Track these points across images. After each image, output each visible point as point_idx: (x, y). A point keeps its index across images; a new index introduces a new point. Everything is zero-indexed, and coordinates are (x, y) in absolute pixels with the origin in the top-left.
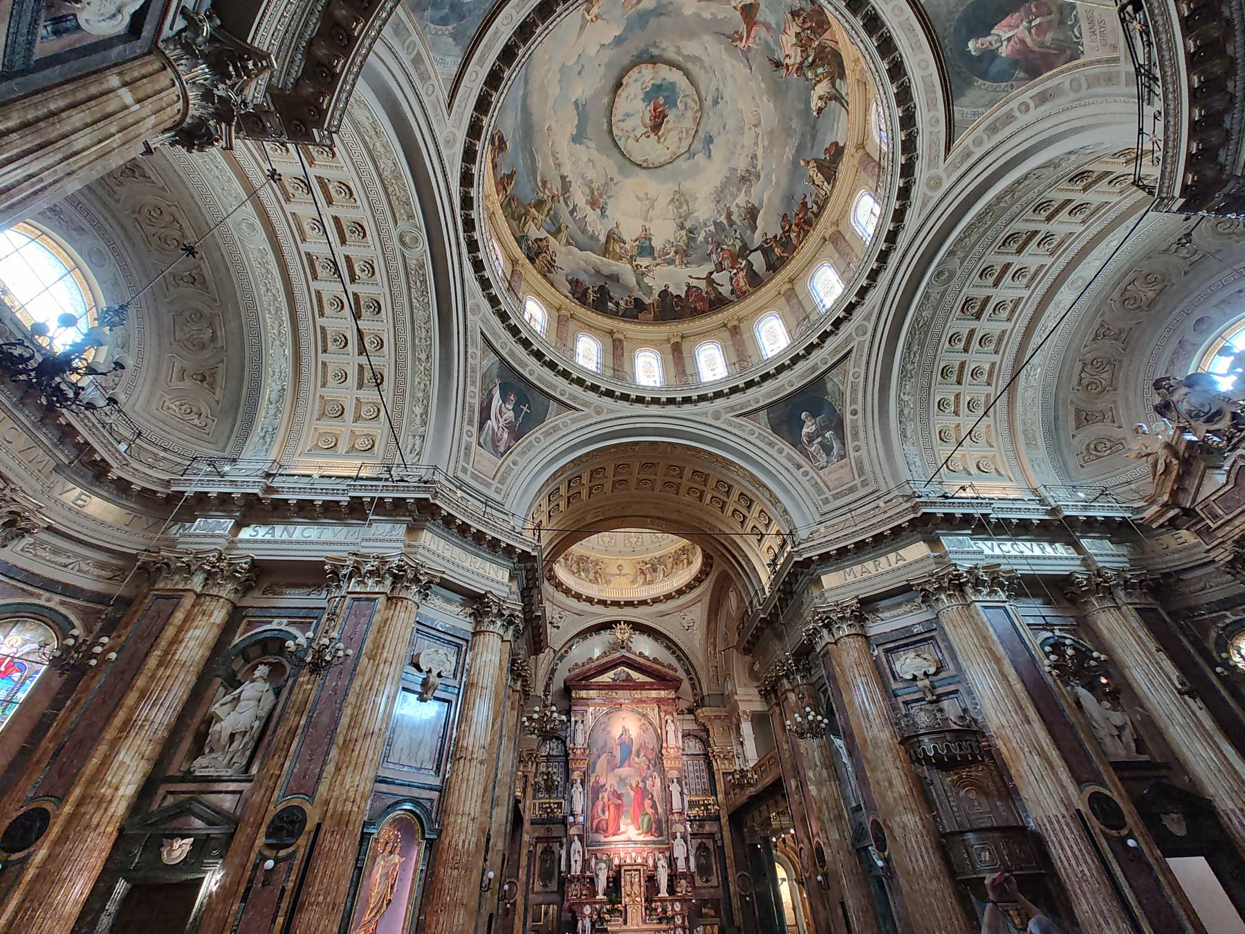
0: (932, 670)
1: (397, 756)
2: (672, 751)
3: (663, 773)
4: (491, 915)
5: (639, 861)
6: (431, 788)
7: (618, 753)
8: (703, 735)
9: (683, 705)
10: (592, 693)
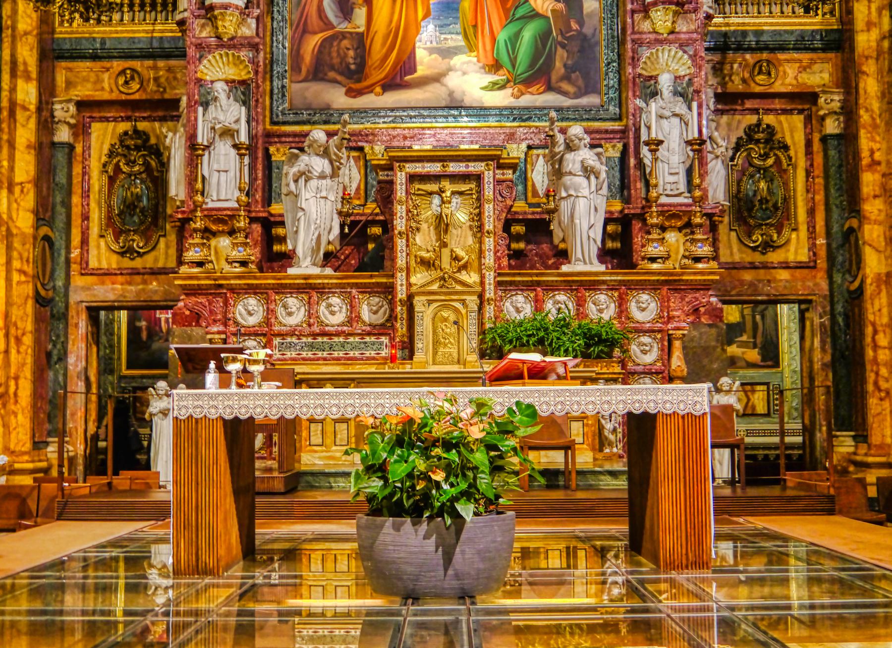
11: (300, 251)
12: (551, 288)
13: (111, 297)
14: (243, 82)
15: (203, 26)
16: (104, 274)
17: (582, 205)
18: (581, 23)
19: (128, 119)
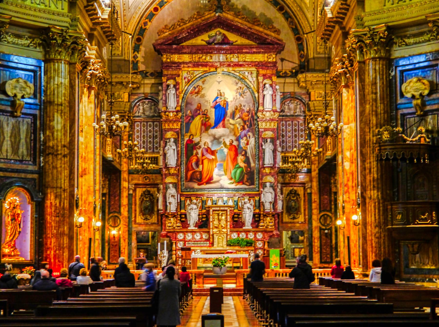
0: (426, 92)
1: (5, 154)
2: (268, 114)
3: (258, 134)
4: (90, 240)
5: (231, 203)
6: (32, 172)
7: (212, 114)
8: (305, 98)
9: (288, 67)
10: (186, 58)
11: (191, 224)
12: (241, 232)
13: (142, 229)
14: (175, 183)
15: (166, 171)
16: (140, 224)
17: (247, 215)
18: (250, 169)
19: (145, 187)
